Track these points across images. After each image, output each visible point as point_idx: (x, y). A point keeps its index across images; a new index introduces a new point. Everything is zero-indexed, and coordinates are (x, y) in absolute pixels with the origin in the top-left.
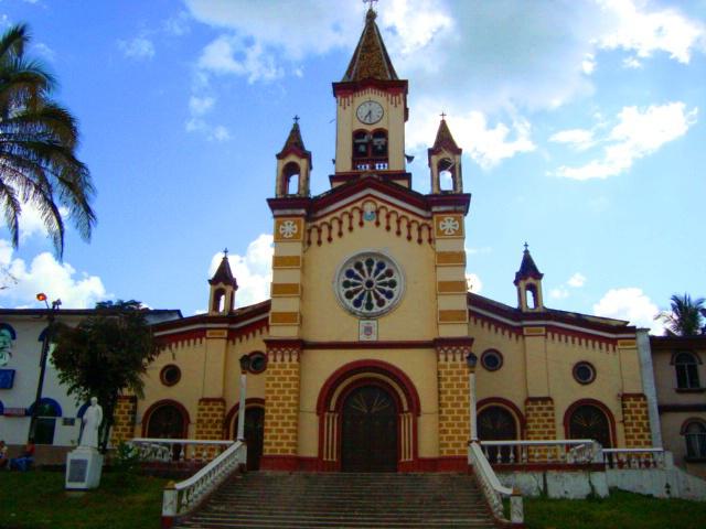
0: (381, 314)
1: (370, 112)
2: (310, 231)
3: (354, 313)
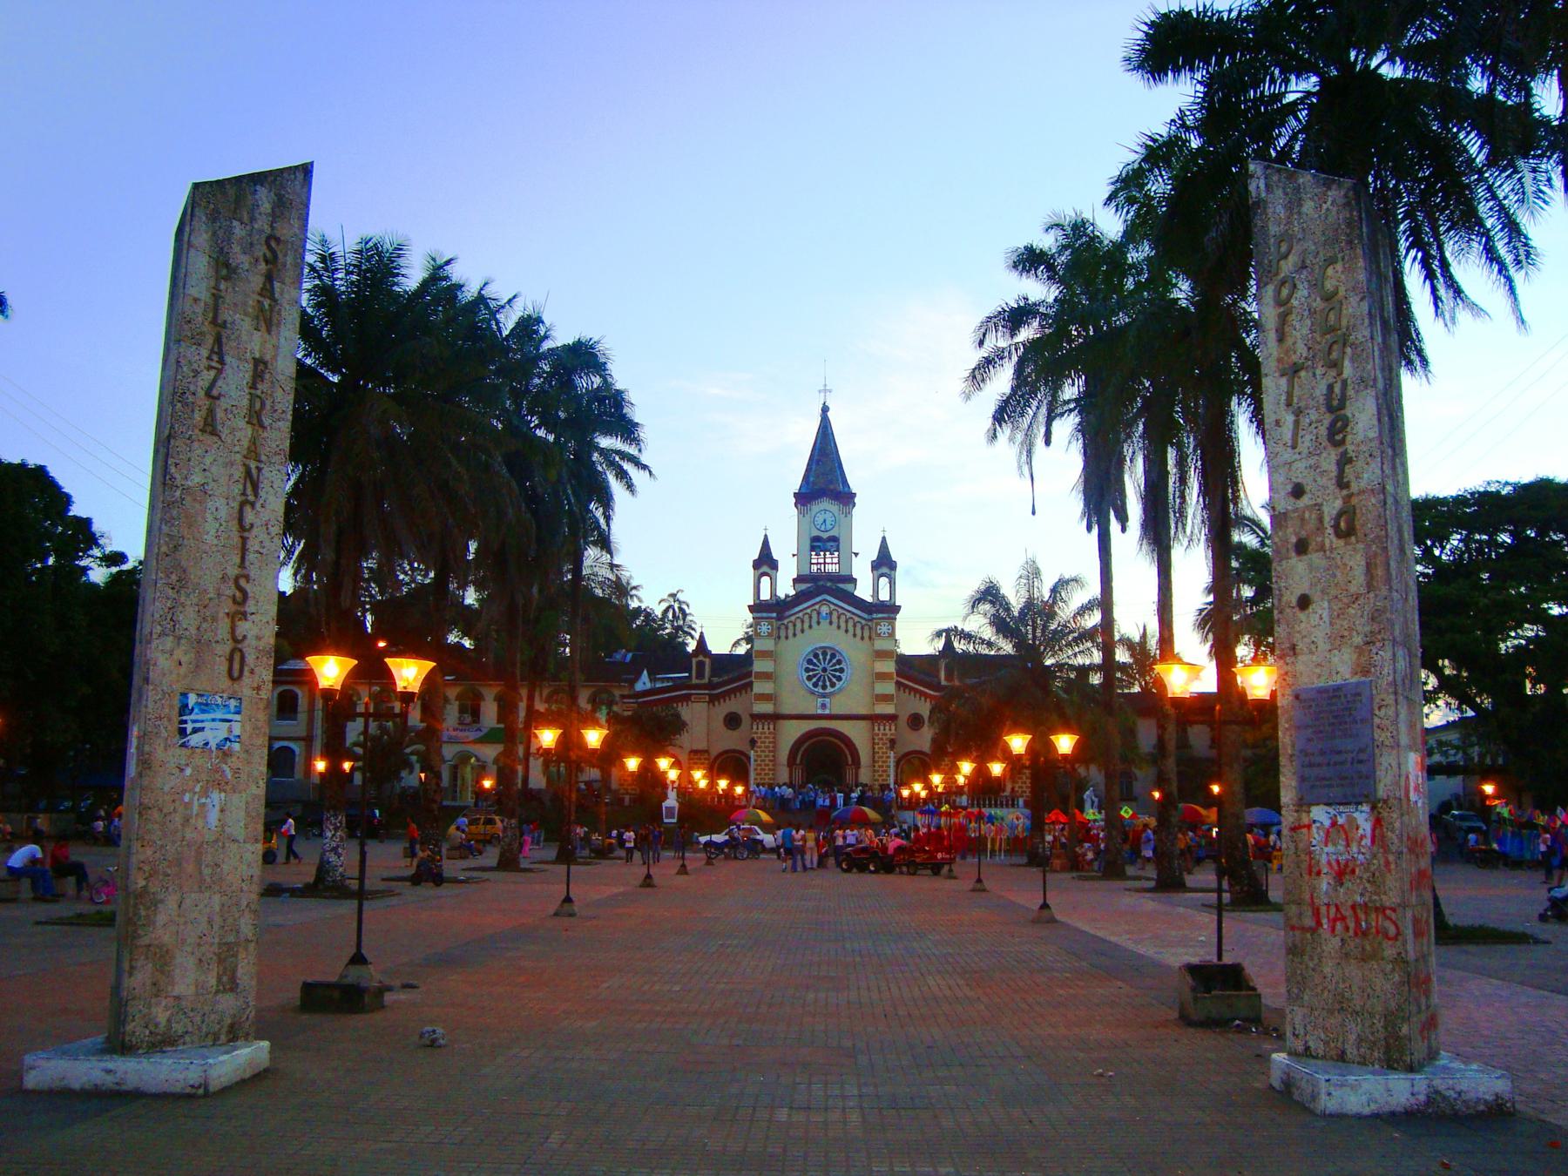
0: (831, 694)
1: (825, 521)
2: (779, 628)
3: (813, 693)
